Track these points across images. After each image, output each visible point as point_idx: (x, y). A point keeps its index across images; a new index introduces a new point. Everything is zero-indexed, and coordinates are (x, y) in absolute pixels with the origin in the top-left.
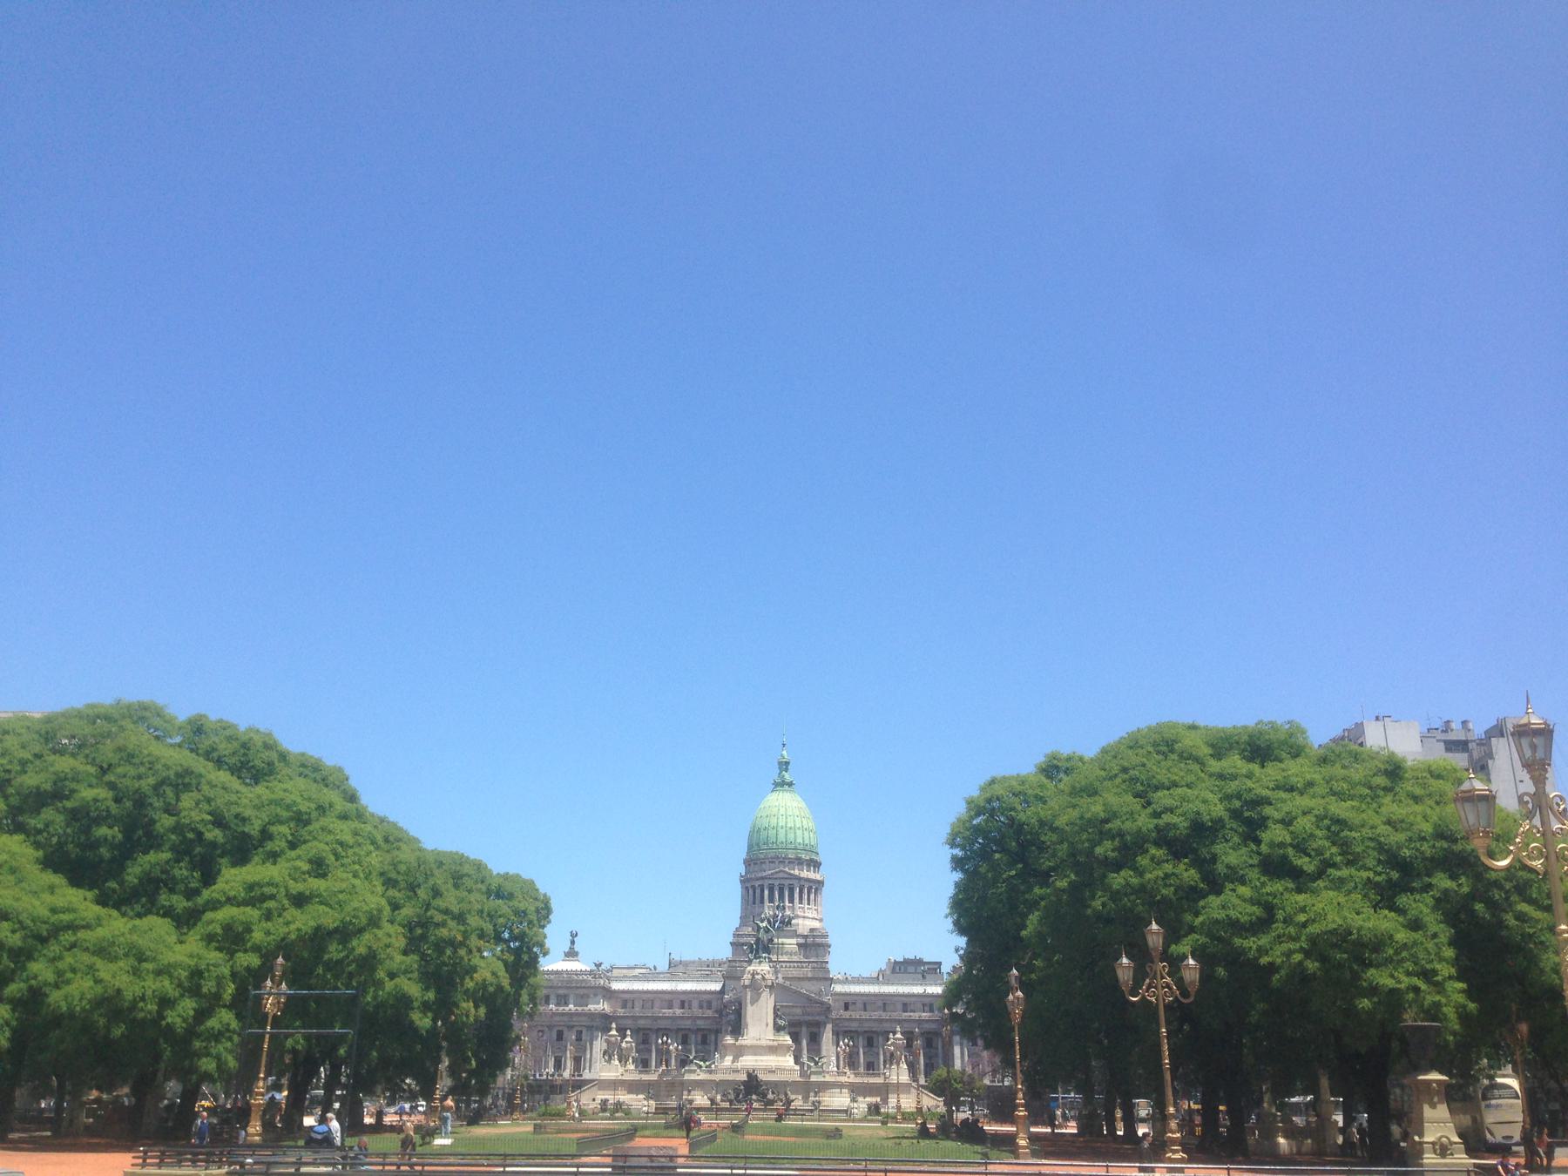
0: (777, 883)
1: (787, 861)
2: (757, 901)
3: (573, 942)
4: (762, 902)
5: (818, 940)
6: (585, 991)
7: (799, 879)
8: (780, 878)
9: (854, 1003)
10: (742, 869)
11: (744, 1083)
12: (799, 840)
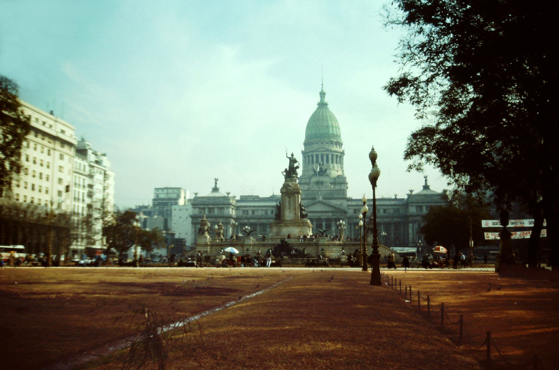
0: (320, 153)
1: (325, 143)
2: (310, 163)
3: (216, 183)
6: (223, 206)
7: (331, 151)
11: (279, 245)
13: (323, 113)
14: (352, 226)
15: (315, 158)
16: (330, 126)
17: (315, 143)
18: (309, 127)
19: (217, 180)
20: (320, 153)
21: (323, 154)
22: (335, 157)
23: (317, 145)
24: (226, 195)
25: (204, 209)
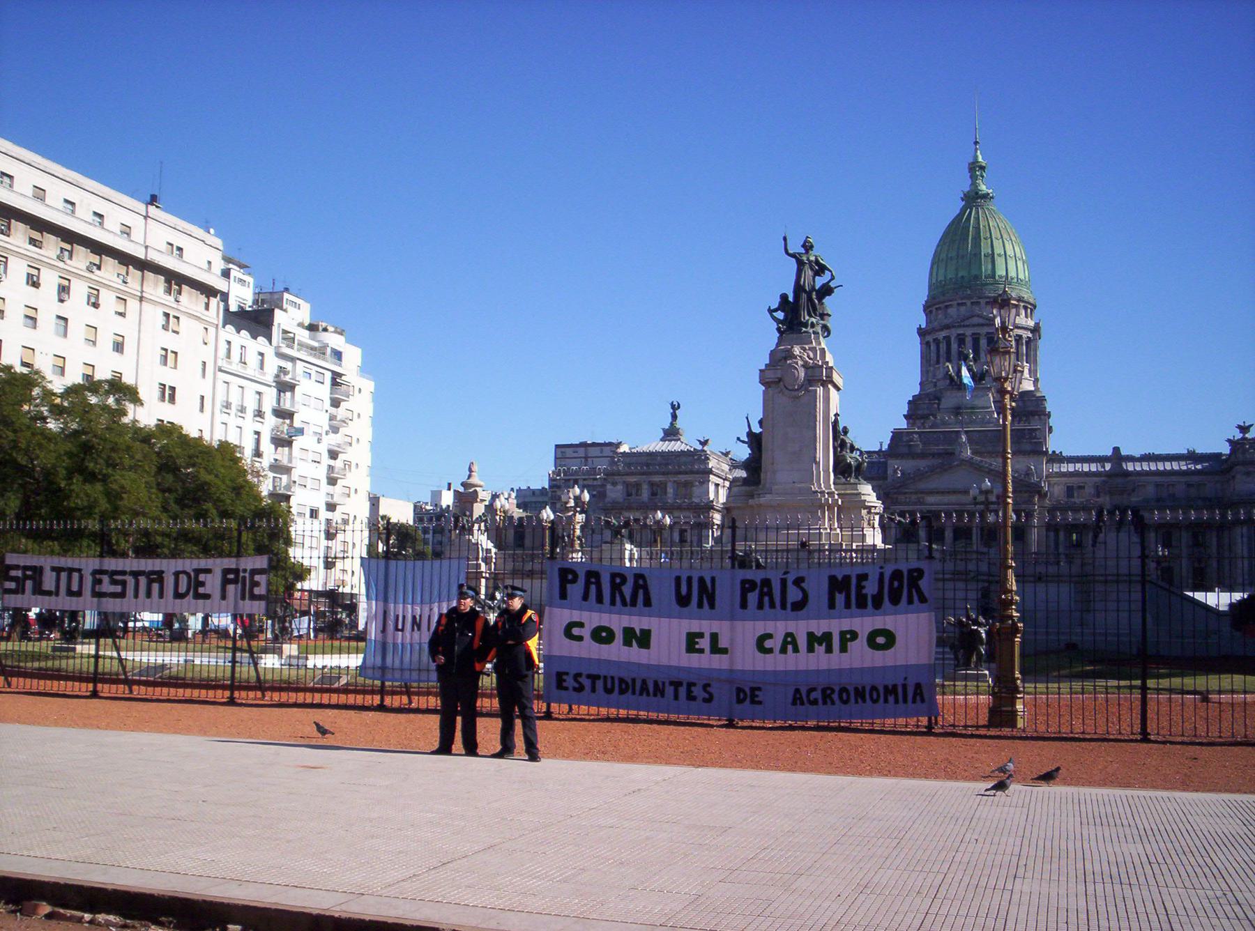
0: (969, 332)
3: (674, 417)
8: (974, 326)
9: (1081, 488)
10: (922, 321)
13: (977, 219)
14: (1062, 535)
15: (954, 346)
16: (999, 255)
17: (955, 302)
18: (936, 261)
19: (679, 407)
20: (969, 332)
21: (979, 334)
23: (963, 309)
24: (699, 447)
25: (638, 486)
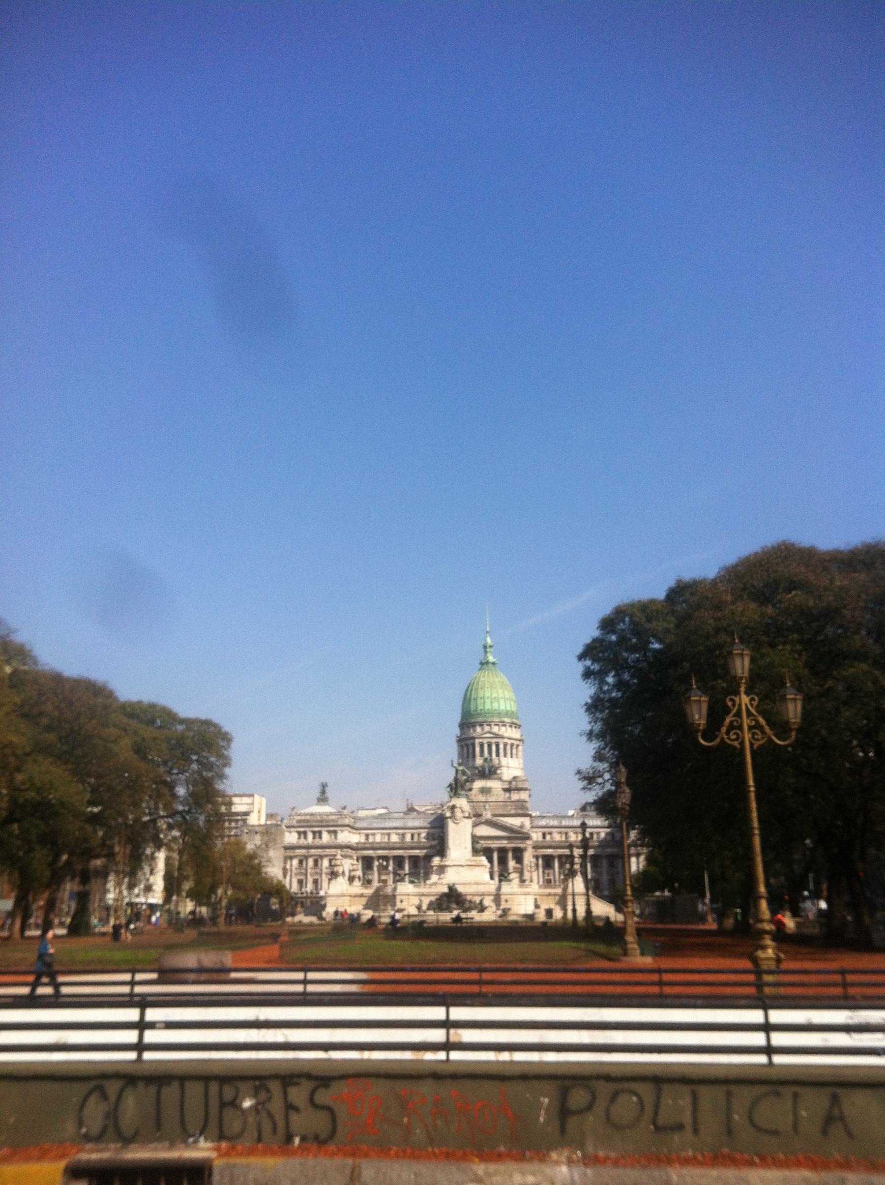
1: (493, 724)
2: (471, 756)
4: (474, 756)
5: (520, 785)
10: (457, 731)
12: (502, 708)
14: (540, 861)
15: (478, 749)
20: (485, 741)
22: (509, 747)
